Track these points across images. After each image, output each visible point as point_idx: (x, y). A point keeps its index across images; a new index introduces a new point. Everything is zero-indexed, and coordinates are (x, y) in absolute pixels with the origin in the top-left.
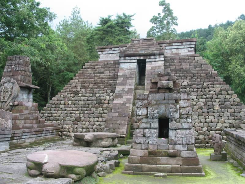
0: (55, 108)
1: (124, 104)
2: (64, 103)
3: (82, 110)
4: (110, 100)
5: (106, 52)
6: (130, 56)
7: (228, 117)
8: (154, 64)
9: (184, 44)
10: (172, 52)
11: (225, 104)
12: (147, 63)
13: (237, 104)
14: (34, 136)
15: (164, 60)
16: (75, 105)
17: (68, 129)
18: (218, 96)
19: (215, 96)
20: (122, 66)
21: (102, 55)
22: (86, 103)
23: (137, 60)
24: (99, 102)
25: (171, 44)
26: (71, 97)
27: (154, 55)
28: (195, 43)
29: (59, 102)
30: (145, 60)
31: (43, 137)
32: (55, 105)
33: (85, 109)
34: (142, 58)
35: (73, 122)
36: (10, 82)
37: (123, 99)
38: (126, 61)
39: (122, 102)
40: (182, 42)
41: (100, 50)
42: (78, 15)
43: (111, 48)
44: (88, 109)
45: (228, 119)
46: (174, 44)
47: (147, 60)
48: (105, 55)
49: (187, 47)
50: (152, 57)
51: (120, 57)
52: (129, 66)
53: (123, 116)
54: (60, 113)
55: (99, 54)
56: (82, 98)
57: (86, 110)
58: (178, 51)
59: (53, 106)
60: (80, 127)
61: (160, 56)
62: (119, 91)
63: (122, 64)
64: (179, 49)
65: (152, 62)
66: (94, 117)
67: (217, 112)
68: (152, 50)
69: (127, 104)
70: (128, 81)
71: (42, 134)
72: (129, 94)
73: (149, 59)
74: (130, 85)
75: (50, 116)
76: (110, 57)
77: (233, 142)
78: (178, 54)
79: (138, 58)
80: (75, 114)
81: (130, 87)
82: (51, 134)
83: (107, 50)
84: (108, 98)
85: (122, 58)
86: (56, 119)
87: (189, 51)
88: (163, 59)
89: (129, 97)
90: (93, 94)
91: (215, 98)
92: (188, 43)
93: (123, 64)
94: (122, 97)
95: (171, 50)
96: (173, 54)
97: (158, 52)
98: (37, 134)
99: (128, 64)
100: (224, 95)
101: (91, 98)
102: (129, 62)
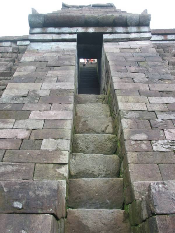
1: (33, 141)
23: (79, 35)
30: (101, 34)
34: (91, 30)
37: (28, 121)
38: (49, 37)
39: (23, 134)
47: (105, 37)
50: (120, 29)
53: (16, 211)
61: (139, 28)
62: (15, 98)
69: (44, 141)
70: (50, 73)
72: (55, 105)
73: (111, 33)
74: (57, 81)
79: (81, 30)
85: (38, 30)
89: (66, 31)
94: (26, 115)
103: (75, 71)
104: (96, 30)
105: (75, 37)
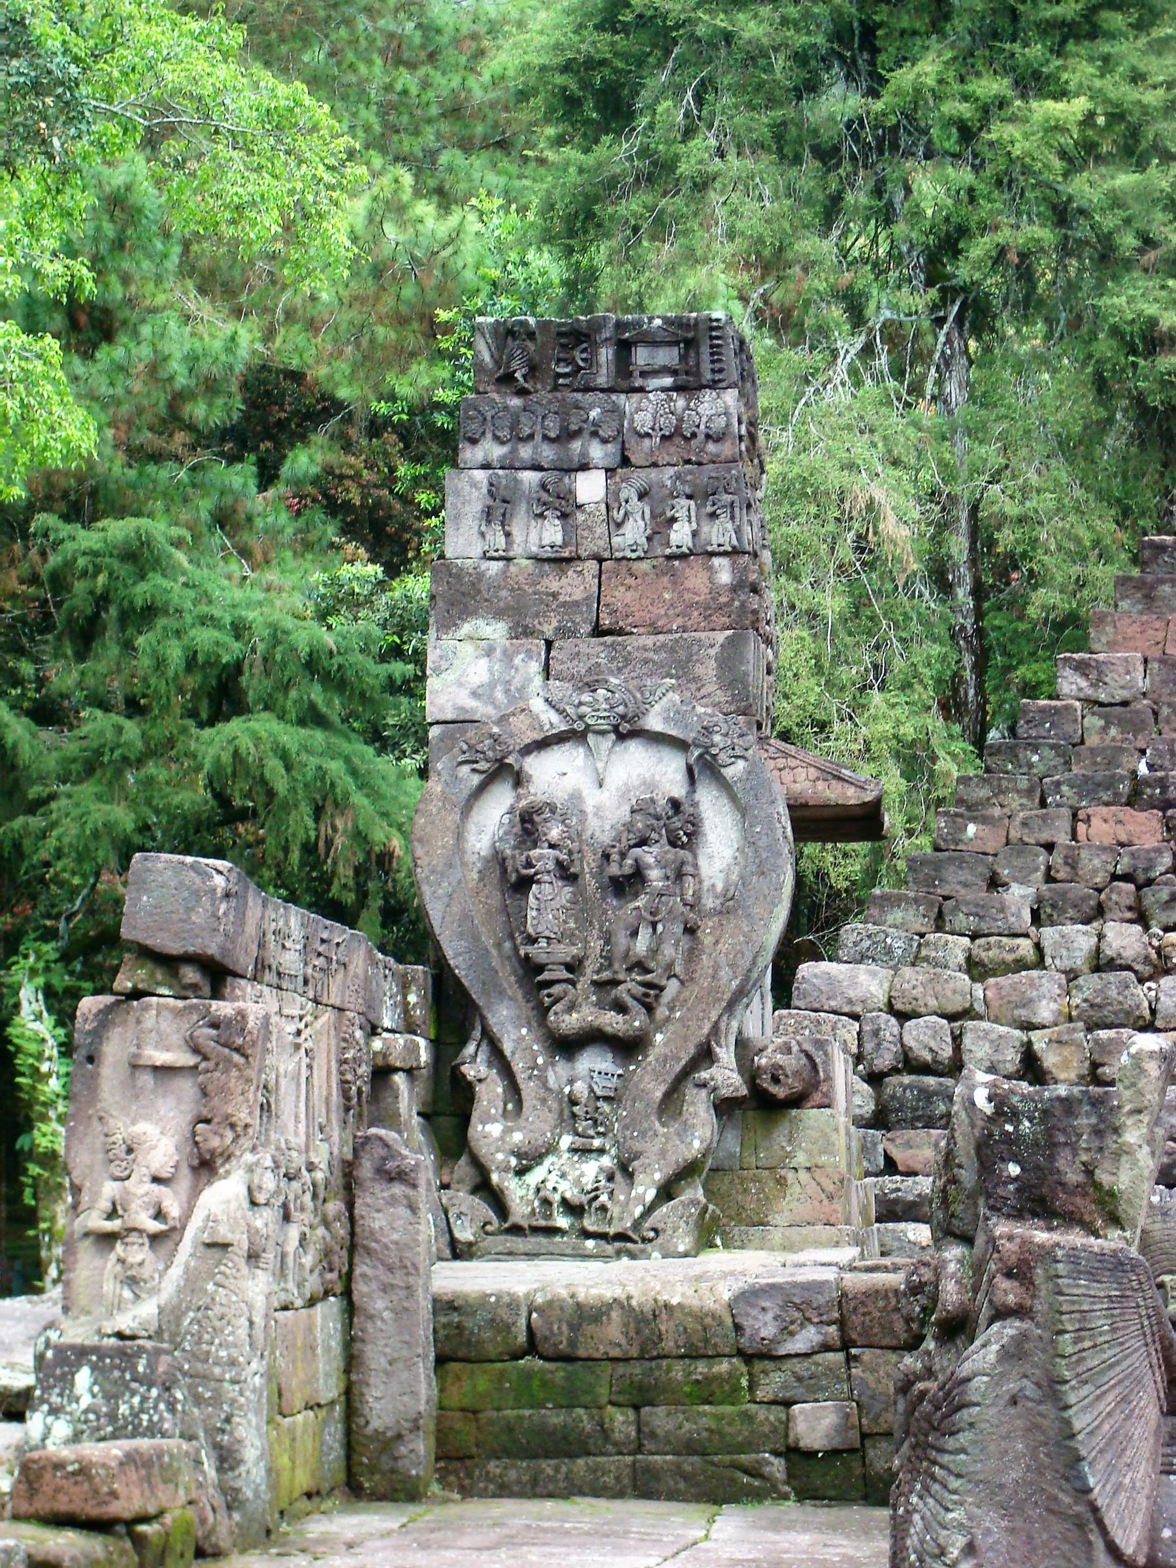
29: (926, 1036)
36: (622, 737)
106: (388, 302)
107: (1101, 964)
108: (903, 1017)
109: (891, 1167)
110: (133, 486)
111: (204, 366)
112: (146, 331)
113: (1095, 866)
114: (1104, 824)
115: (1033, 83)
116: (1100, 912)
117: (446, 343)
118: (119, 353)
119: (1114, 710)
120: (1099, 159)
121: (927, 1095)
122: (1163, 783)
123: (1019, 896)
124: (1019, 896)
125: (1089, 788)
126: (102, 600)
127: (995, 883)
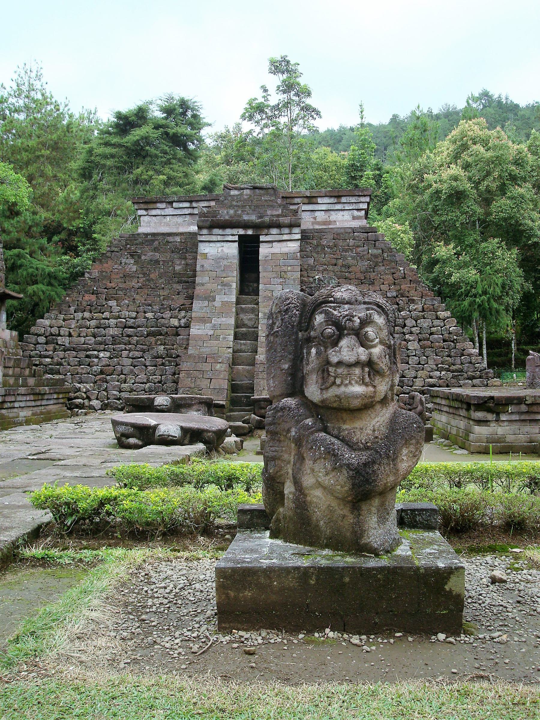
0: (46, 343)
2: (67, 334)
3: (114, 350)
4: (180, 326)
5: (158, 212)
6: (224, 225)
7: (437, 365)
8: (278, 248)
9: (344, 200)
10: (315, 218)
11: (431, 339)
12: (261, 245)
13: (456, 340)
14: (29, 404)
15: (301, 240)
16: (95, 338)
17: (85, 393)
18: (416, 321)
19: (410, 322)
20: (203, 248)
21: (146, 219)
22: (122, 334)
23: (240, 236)
24: (153, 332)
25: (314, 200)
26: (83, 319)
27: (279, 226)
28: (367, 199)
29: (55, 330)
30: (258, 237)
31: (43, 408)
32: (46, 337)
33: (123, 346)
34: (250, 232)
35: (95, 376)
38: (214, 238)
40: (339, 197)
41: (142, 206)
42: (37, 85)
43: (171, 203)
44: (130, 346)
45: (437, 370)
46: (320, 200)
47: (262, 238)
48: (154, 218)
49: (351, 208)
50: (274, 231)
51: (200, 228)
52: (220, 251)
54: (62, 356)
55: (140, 216)
56: (113, 322)
57: (126, 350)
58: (329, 216)
59: (42, 339)
60: (114, 387)
63: (204, 244)
64: (332, 212)
65: (272, 242)
66: (146, 366)
67: (415, 356)
68: (271, 214)
71: (42, 399)
75: (37, 363)
76: (168, 225)
77: (445, 409)
78: (330, 223)
79: (241, 232)
80: (97, 357)
81: (226, 299)
82: (55, 401)
83: (159, 205)
84: (175, 322)
85: (205, 231)
86: (52, 369)
87: (354, 218)
88: (298, 236)
90: (138, 313)
91: (411, 325)
92: (353, 199)
93: (207, 244)
95: (312, 213)
96: (319, 223)
97: (286, 220)
98: (35, 400)
99: (218, 244)
100: (430, 320)
101: (134, 323)
102: (219, 239)
103: (237, 285)
104: (253, 232)
105: (236, 238)
106: (72, 209)
107: (83, 319)
108: (51, 327)
109: (46, 350)
110: (25, 243)
111: (35, 221)
112: (23, 215)
113: (84, 303)
114: (87, 297)
115: (159, 173)
116: (85, 311)
117: (82, 216)
118: (18, 219)
119: (93, 280)
120: (172, 185)
121: (53, 339)
122: (97, 290)
123: (72, 309)
124: (72, 309)
125: (86, 292)
126: (13, 264)
127: (70, 307)
